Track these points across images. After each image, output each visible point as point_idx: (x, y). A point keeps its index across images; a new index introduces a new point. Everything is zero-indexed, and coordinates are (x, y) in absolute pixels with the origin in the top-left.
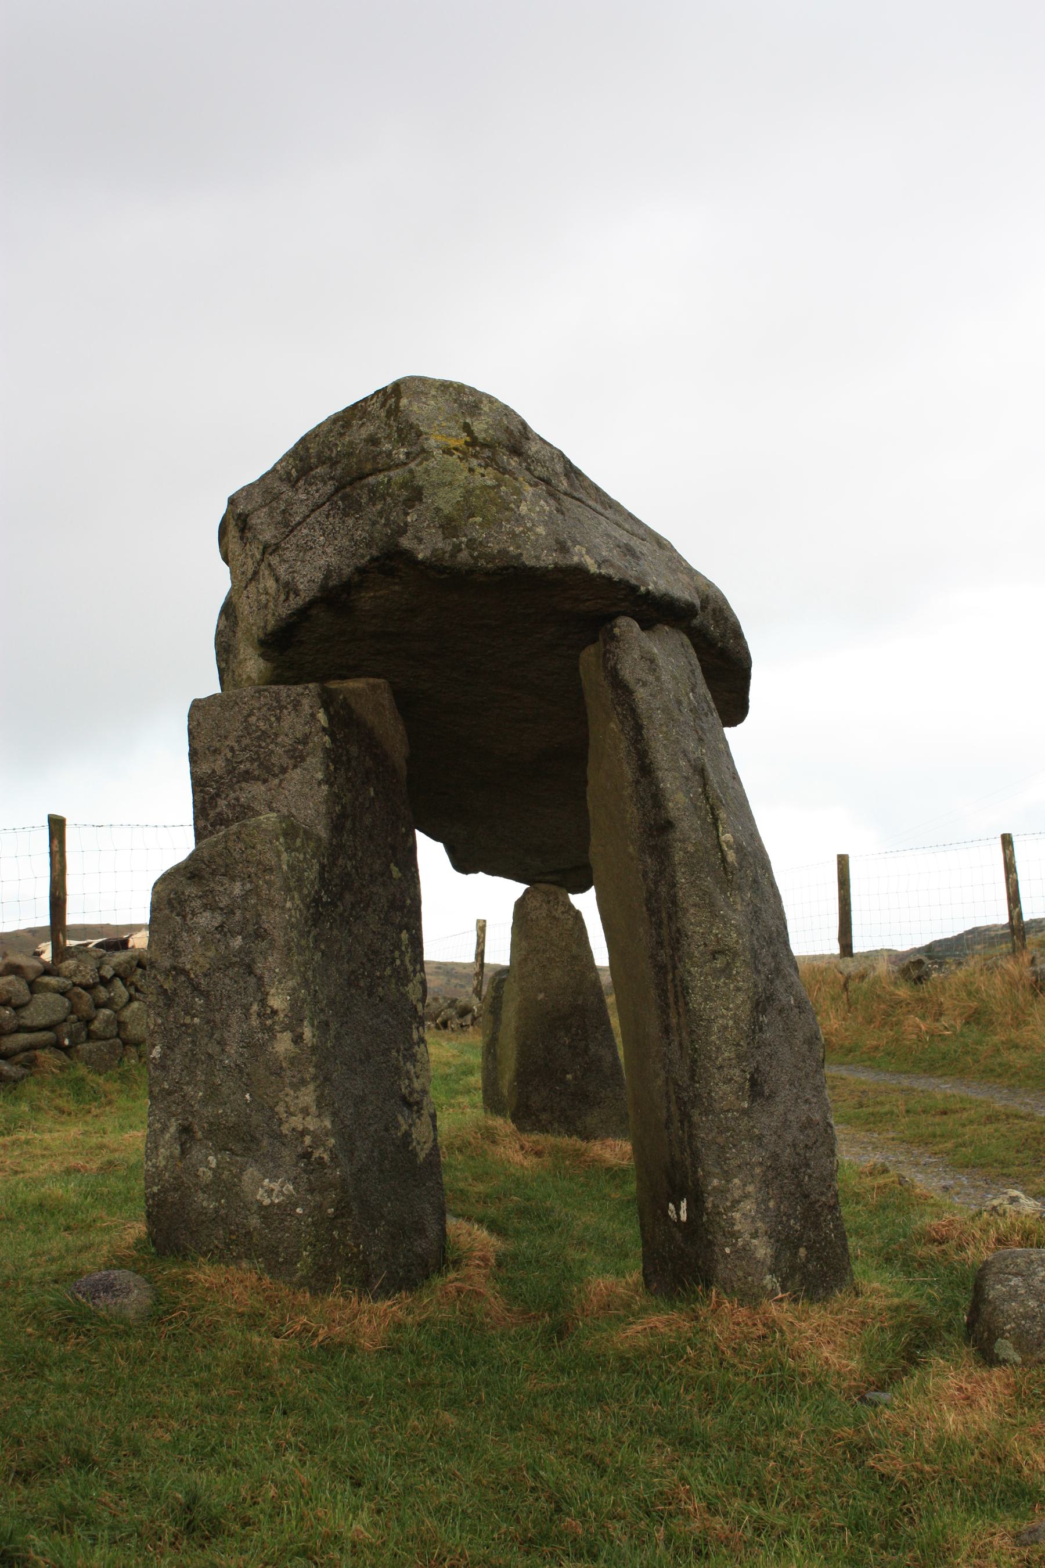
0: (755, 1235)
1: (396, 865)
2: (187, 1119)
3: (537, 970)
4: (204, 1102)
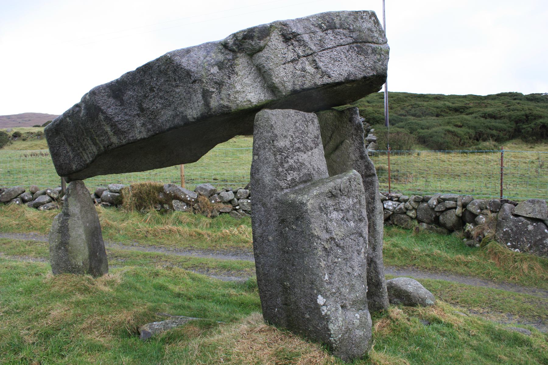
2: (343, 302)
4: (349, 293)
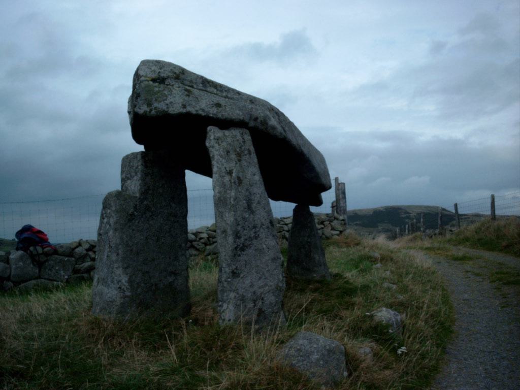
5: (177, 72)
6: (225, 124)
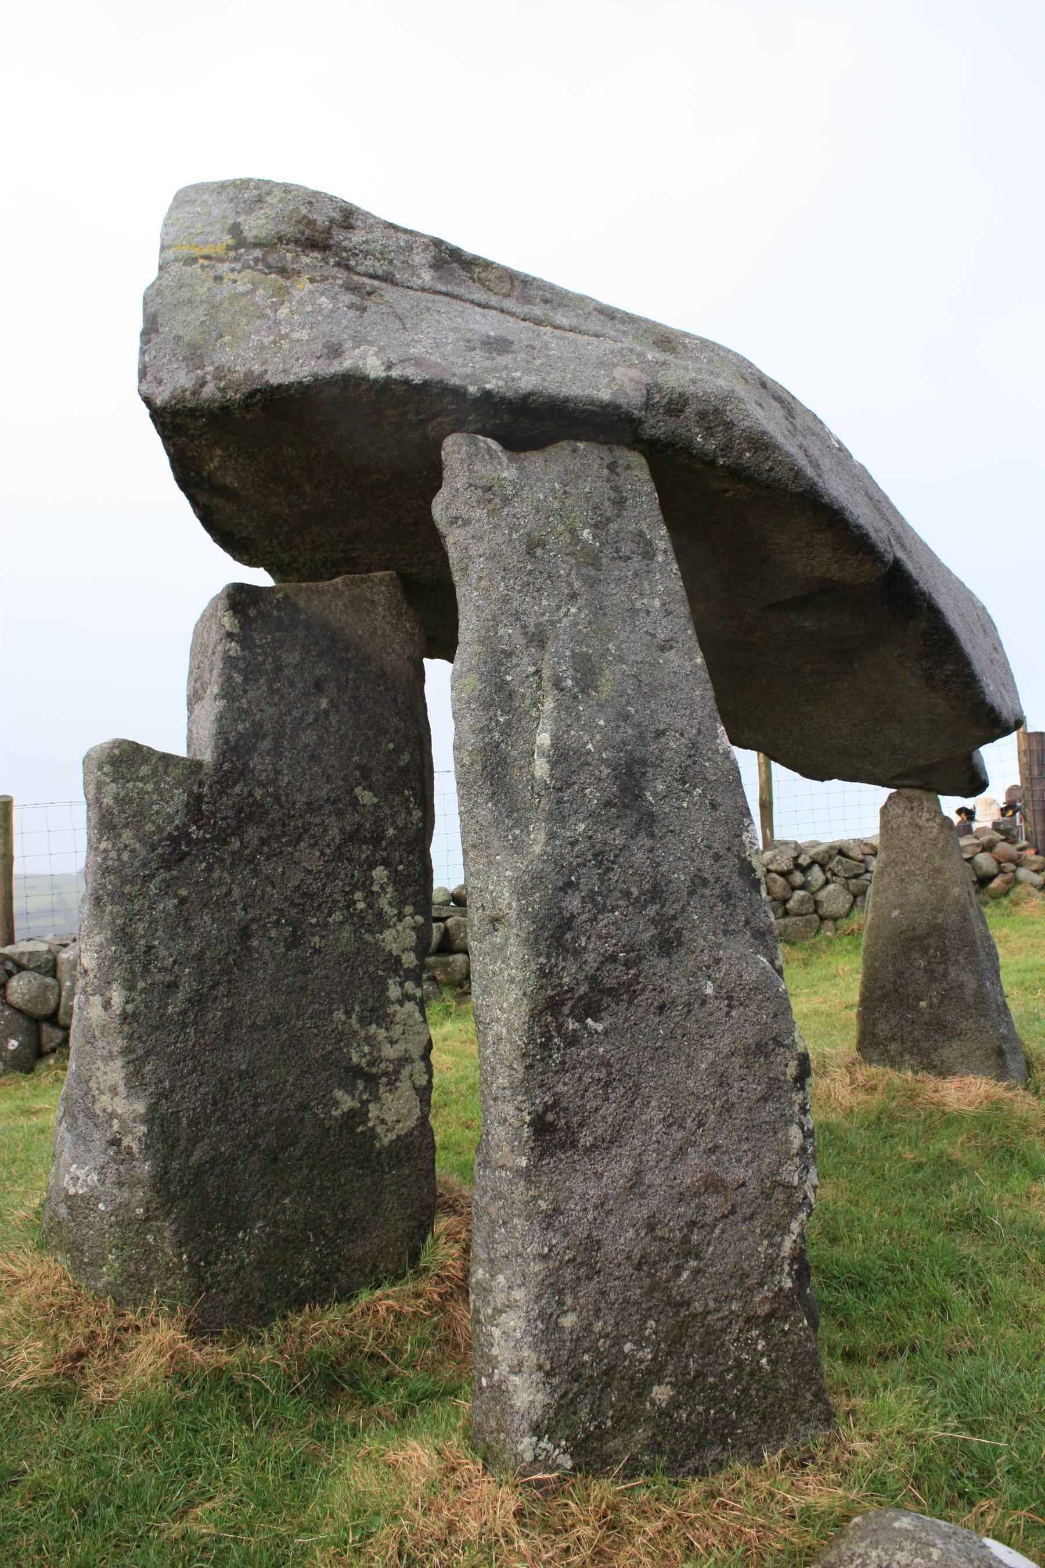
0: (517, 1369)
1: (370, 788)
3: (893, 885)
5: (321, 220)
6: (529, 423)
